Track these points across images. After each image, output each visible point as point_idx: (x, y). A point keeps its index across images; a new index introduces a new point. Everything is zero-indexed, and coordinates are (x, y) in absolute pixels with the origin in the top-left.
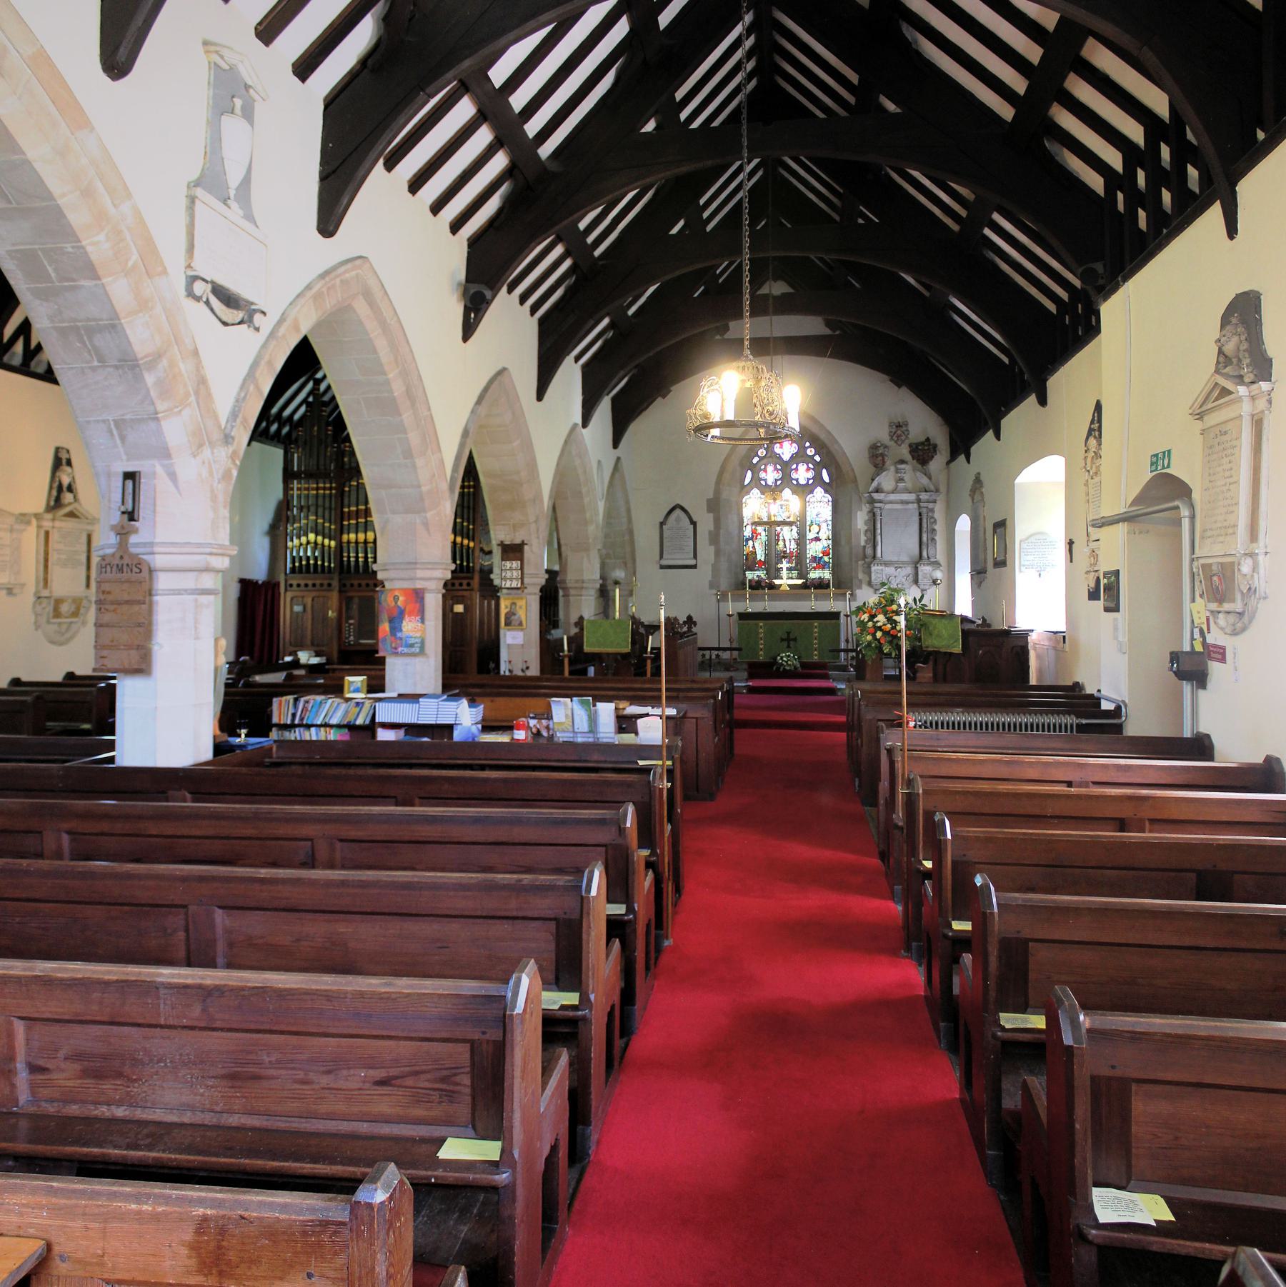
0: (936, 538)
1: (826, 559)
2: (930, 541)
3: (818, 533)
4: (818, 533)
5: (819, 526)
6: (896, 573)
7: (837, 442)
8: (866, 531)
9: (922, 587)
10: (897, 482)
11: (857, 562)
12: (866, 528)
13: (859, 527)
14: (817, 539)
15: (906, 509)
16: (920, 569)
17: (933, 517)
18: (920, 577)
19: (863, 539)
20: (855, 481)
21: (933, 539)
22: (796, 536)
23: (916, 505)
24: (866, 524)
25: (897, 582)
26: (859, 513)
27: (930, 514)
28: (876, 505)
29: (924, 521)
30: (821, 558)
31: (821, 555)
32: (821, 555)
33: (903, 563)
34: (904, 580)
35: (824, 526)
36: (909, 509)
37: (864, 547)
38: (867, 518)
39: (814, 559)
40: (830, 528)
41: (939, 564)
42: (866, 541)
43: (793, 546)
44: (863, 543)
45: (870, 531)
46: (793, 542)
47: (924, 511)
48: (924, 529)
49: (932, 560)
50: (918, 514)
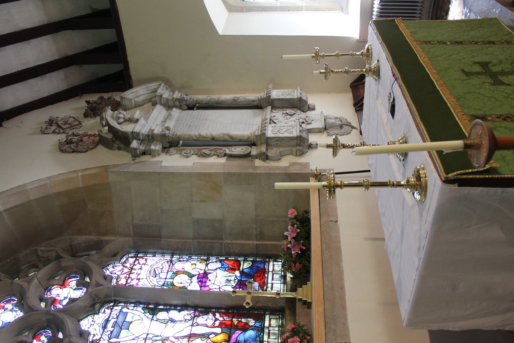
1: (246, 266)
3: (191, 276)
4: (191, 276)
5: (177, 273)
7: (25, 184)
13: (191, 164)
14: (203, 278)
19: (213, 160)
20: (106, 168)
22: (185, 314)
30: (242, 273)
31: (237, 273)
32: (237, 273)
35: (178, 266)
39: (241, 284)
40: (185, 257)
43: (208, 319)
44: (223, 160)
46: (201, 320)
50: (190, 112)
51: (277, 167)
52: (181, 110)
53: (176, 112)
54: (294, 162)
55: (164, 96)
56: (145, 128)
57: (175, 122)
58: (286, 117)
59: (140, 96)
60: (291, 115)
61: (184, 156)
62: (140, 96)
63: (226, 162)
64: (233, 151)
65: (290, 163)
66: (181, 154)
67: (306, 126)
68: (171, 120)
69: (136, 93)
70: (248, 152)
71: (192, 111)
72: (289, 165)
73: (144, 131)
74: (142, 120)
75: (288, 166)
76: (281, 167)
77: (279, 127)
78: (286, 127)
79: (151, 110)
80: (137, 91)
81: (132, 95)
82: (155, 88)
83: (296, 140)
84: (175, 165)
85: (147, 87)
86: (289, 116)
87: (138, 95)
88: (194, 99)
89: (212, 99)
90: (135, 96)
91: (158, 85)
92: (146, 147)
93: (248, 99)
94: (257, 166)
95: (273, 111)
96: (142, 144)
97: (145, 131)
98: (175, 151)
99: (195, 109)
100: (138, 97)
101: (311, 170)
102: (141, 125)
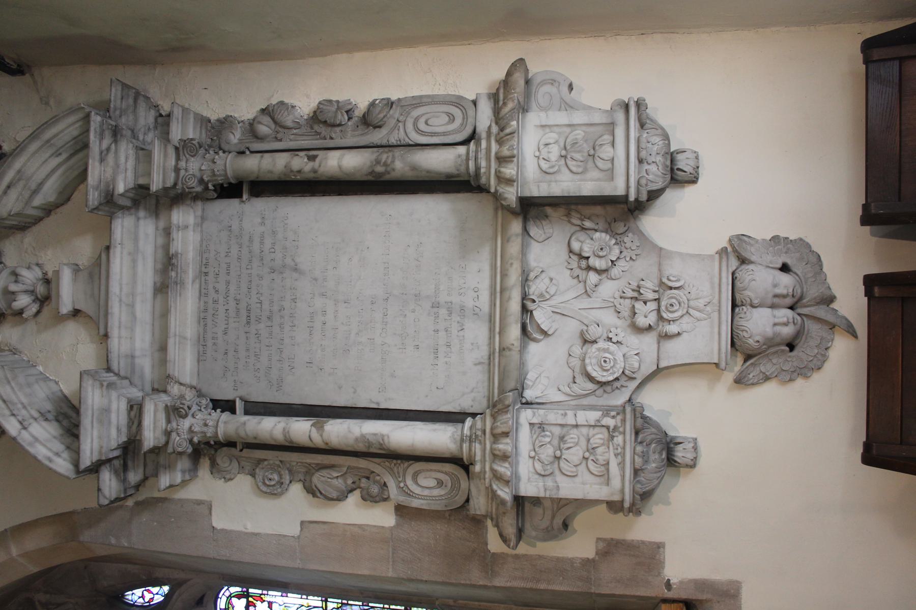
0: (362, 105)
2: (377, 137)
6: (569, 329)
8: (312, 491)
9: (655, 174)
10: (60, 319)
11: (491, 562)
12: (296, 490)
13: (295, 530)
15: (203, 274)
16: (537, 189)
17: (251, 128)
18: (589, 187)
21: (368, 121)
23: (182, 216)
24: (274, 491)
25: (622, 333)
26: (219, 522)
27: (235, 138)
28: (150, 437)
29: (252, 165)
33: (499, 273)
34: (608, 289)
36: (202, 252)
37: (401, 510)
38: (243, 484)
41: (506, 83)
42: (369, 498)
45: (310, 471)
47: (194, 166)
48: (300, 163)
49: (484, 118)
50: (231, 206)
51: (558, 560)
52: (199, 204)
53: (186, 227)
54: (612, 539)
55: (121, 188)
56: (113, 417)
57: (197, 286)
58: (583, 274)
59: (41, 185)
60: (599, 272)
61: (266, 493)
62: (41, 185)
63: (398, 525)
64: (409, 494)
65: (598, 539)
66: (253, 475)
67: (659, 343)
68: (182, 283)
69: (22, 183)
70: (460, 500)
71: (235, 202)
72: (597, 554)
73: (114, 432)
74: (90, 389)
75: (593, 560)
76: (571, 561)
77: (557, 431)
78: (584, 431)
79: (104, 256)
80: (19, 171)
81: (13, 194)
82: (76, 133)
83: (621, 414)
84: (251, 528)
85: (48, 141)
86: (593, 277)
87: (33, 186)
88: (225, 170)
89: (292, 171)
90: (27, 194)
91: (80, 123)
92: (145, 466)
93: (428, 172)
94: (494, 554)
95: (534, 231)
96: (130, 463)
97: (119, 430)
98: (235, 464)
99: (245, 196)
100: (35, 192)
101: (668, 585)
102: (95, 417)
